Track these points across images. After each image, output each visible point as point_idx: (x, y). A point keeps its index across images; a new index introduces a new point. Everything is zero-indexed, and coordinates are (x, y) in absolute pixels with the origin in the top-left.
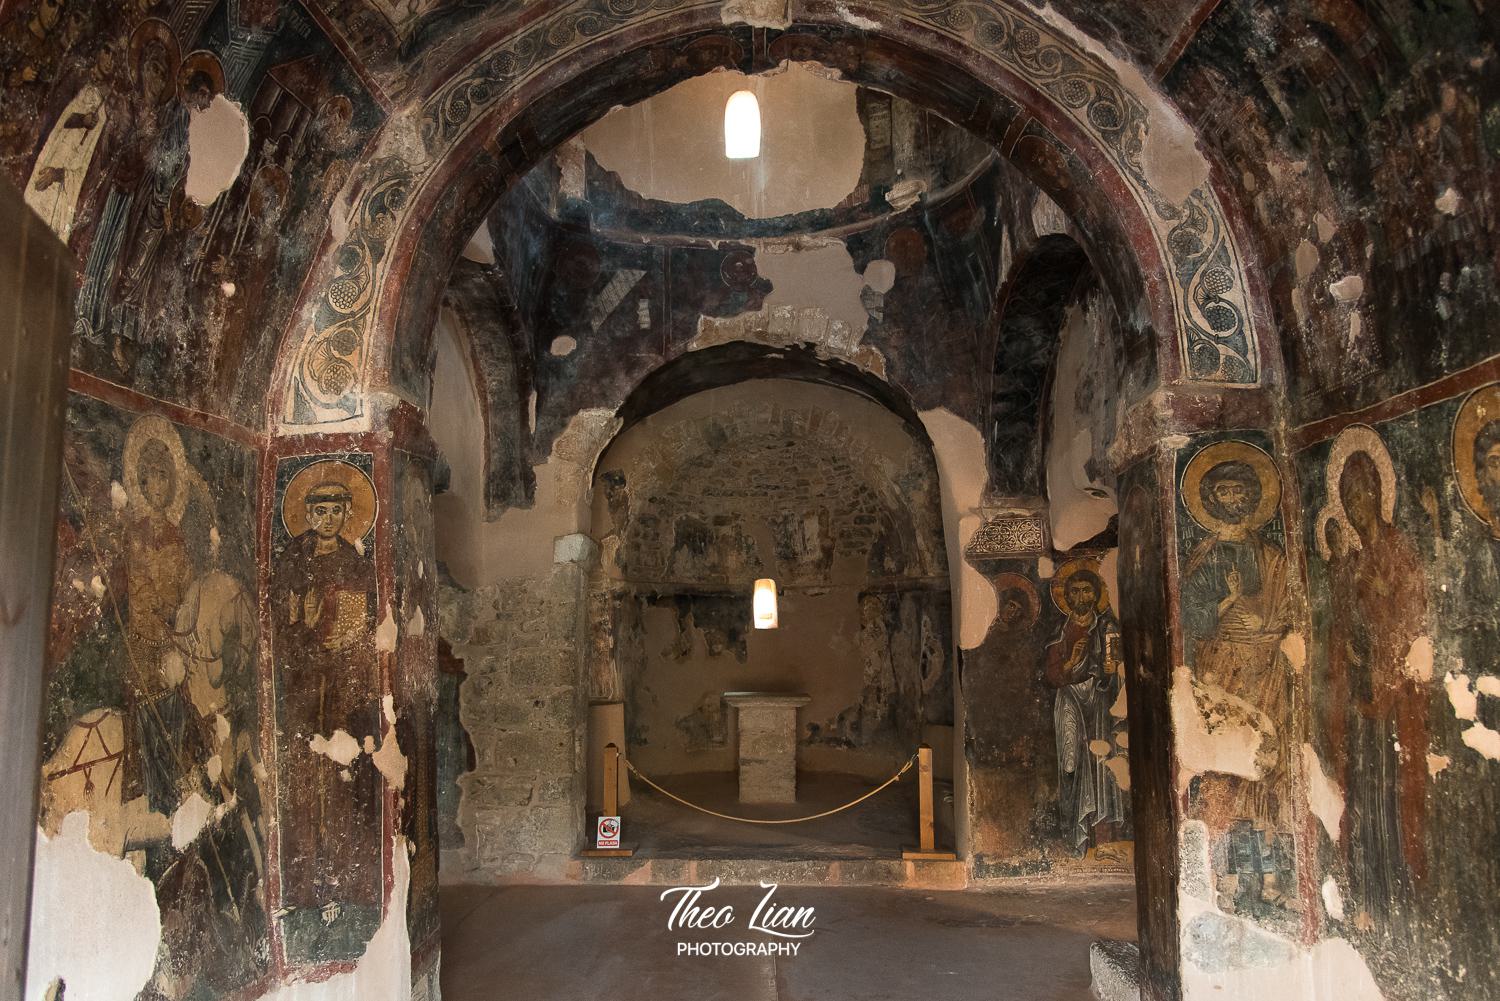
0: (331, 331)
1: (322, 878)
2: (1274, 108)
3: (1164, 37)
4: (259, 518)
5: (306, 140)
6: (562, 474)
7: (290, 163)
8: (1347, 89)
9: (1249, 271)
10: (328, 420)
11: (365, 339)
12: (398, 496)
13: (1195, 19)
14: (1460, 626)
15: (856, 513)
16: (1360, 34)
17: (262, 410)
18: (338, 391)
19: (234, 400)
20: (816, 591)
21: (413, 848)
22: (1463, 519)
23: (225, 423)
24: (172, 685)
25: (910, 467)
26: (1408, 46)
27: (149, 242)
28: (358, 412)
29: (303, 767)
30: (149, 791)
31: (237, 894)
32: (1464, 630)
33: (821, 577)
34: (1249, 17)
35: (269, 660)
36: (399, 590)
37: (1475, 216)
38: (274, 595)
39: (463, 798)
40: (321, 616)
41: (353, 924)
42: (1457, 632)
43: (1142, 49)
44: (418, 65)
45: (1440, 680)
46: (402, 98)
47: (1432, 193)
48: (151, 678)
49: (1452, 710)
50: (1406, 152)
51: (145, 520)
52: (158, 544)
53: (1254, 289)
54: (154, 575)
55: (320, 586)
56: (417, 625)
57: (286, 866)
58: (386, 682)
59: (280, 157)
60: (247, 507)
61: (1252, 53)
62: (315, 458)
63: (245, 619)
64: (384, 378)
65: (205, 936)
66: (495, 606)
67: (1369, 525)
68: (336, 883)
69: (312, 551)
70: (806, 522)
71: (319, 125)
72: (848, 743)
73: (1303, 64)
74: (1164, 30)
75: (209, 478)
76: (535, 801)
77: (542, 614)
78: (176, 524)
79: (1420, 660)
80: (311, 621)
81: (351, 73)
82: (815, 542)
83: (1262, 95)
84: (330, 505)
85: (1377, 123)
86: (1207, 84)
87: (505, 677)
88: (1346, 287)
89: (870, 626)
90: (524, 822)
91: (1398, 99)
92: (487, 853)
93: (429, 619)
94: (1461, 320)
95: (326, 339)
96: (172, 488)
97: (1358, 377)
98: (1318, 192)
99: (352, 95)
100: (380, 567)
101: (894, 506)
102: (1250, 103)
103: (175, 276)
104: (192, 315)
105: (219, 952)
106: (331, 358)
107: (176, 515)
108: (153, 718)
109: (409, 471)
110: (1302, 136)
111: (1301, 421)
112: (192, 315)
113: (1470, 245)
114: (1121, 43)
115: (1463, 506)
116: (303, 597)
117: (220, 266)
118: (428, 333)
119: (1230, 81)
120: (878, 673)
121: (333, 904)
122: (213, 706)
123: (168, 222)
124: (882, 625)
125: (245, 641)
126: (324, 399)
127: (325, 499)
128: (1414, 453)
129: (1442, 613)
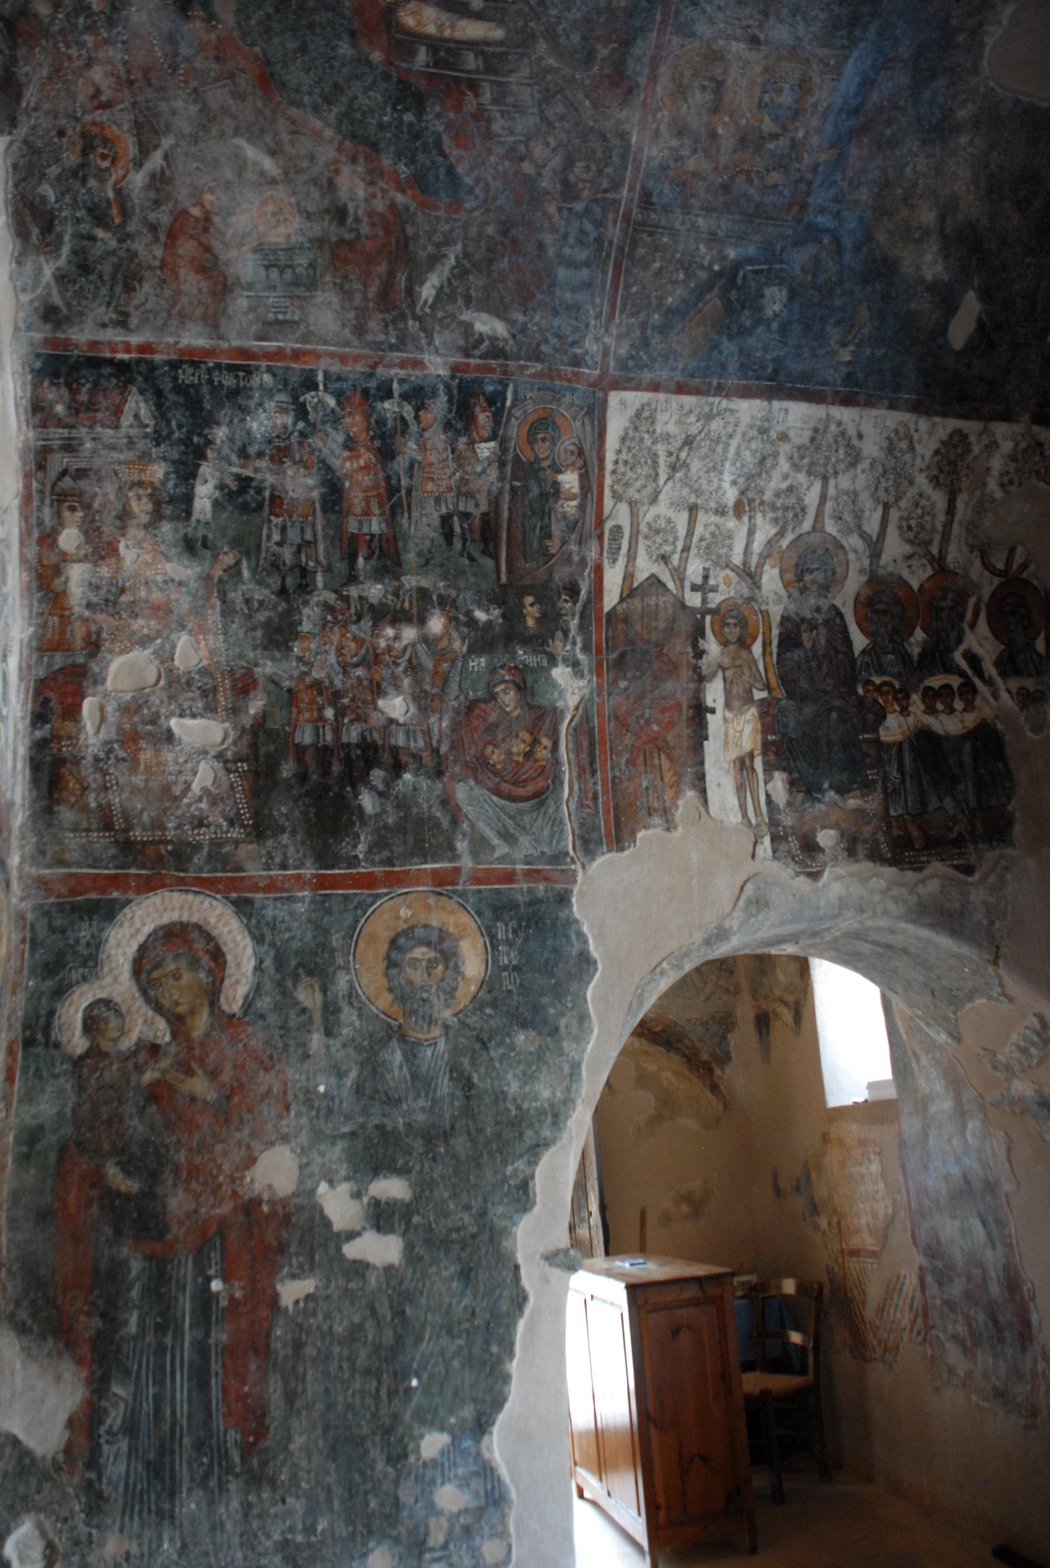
2: (188, 499)
3: (123, 322)
8: (311, 544)
13: (191, 351)
14: (346, 1129)
16: (367, 513)
22: (360, 1016)
26: (410, 557)
32: (353, 1134)
34: (261, 404)
37: (428, 733)
42: (342, 1136)
43: (68, 305)
45: (312, 1192)
47: (377, 690)
49: (327, 1223)
50: (359, 642)
53: (20, 668)
61: (221, 433)
67: (192, 1012)
73: (273, 488)
74: (134, 321)
79: (275, 1172)
83: (187, 472)
85: (331, 597)
86: (118, 412)
88: (200, 733)
91: (375, 591)
94: (390, 820)
97: (205, 836)
98: (197, 612)
102: (158, 471)
110: (205, 545)
111: (61, 862)
113: (416, 757)
114: (48, 272)
115: (361, 1002)
119: (156, 431)
128: (292, 938)
129: (317, 1117)
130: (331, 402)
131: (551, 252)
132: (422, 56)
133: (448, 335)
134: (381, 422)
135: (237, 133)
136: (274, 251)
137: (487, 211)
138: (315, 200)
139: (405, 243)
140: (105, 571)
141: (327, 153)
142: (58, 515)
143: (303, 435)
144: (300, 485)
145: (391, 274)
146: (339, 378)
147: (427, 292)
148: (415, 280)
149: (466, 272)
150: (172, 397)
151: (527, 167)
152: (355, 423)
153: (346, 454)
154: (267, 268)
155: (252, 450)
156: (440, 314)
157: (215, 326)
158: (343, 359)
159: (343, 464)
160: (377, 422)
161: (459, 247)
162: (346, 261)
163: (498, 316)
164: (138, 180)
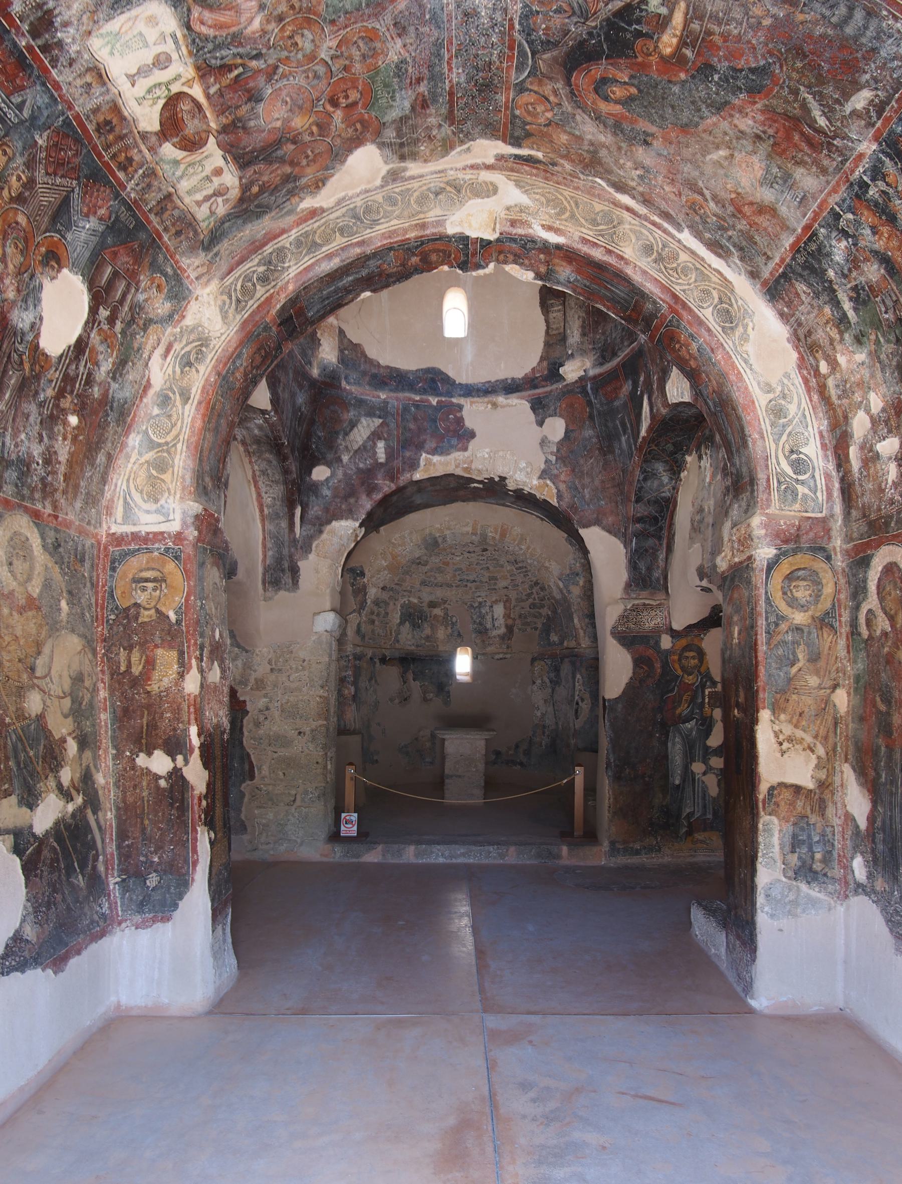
0: (150, 456)
1: (146, 856)
2: (845, 315)
4: (97, 593)
5: (130, 309)
6: (319, 569)
7: (119, 326)
9: (821, 433)
10: (148, 521)
11: (176, 461)
12: (201, 579)
13: (792, 246)
15: (531, 600)
17: (99, 513)
18: (156, 501)
19: (78, 504)
20: (501, 656)
21: (213, 835)
23: (71, 523)
24: (33, 715)
25: (571, 569)
27: (12, 382)
28: (171, 517)
29: (130, 777)
30: (17, 792)
31: (83, 866)
33: (504, 646)
35: (105, 699)
36: (202, 648)
38: (108, 650)
39: (246, 800)
40: (144, 667)
41: (169, 889)
44: (216, 255)
46: (204, 279)
48: (17, 709)
51: (12, 593)
52: (22, 610)
53: (824, 446)
54: (19, 633)
55: (143, 645)
56: (215, 675)
57: (119, 847)
58: (192, 716)
59: (111, 320)
60: (88, 584)
61: (831, 273)
62: (138, 550)
63: (87, 668)
64: (190, 493)
65: (59, 897)
66: (270, 662)
68: (156, 859)
69: (137, 619)
70: (495, 607)
71: (141, 297)
72: (521, 764)
74: (769, 253)
75: (60, 562)
76: (298, 803)
77: (304, 669)
78: (35, 596)
80: (136, 670)
81: (166, 258)
82: (501, 621)
83: (837, 304)
84: (150, 585)
86: (798, 295)
87: (277, 714)
89: (539, 681)
90: (290, 817)
92: (263, 839)
93: (223, 671)
95: (147, 462)
96: (32, 568)
98: (872, 376)
99: (165, 275)
100: (188, 632)
101: (558, 597)
102: (827, 310)
103: (33, 408)
104: (46, 439)
105: (69, 909)
106: (150, 476)
107: (35, 589)
108: (19, 739)
109: (209, 561)
112: (46, 439)
116: (131, 651)
117: (66, 403)
118: (223, 459)
120: (543, 715)
121: (154, 874)
122: (64, 731)
123: (27, 366)
124: (547, 681)
125: (87, 683)
126: (146, 506)
127: (147, 580)
130: (850, 216)
131: (830, 32)
132: (688, 52)
133: (854, 127)
134: (876, 204)
135: (704, 156)
136: (765, 178)
137: (785, 60)
138: (747, 144)
139: (787, 116)
140: (838, 376)
141: (725, 125)
142: (815, 357)
143: (855, 245)
144: (873, 272)
145: (802, 134)
146: (844, 201)
147: (822, 122)
148: (812, 124)
149: (820, 93)
150: (805, 273)
151: (767, 22)
152: (867, 217)
153: (877, 237)
154: (772, 187)
155: (846, 271)
156: (839, 124)
157: (788, 228)
158: (835, 190)
159: (879, 245)
160: (875, 206)
161: (802, 88)
162: (784, 151)
163: (859, 90)
164: (712, 204)
